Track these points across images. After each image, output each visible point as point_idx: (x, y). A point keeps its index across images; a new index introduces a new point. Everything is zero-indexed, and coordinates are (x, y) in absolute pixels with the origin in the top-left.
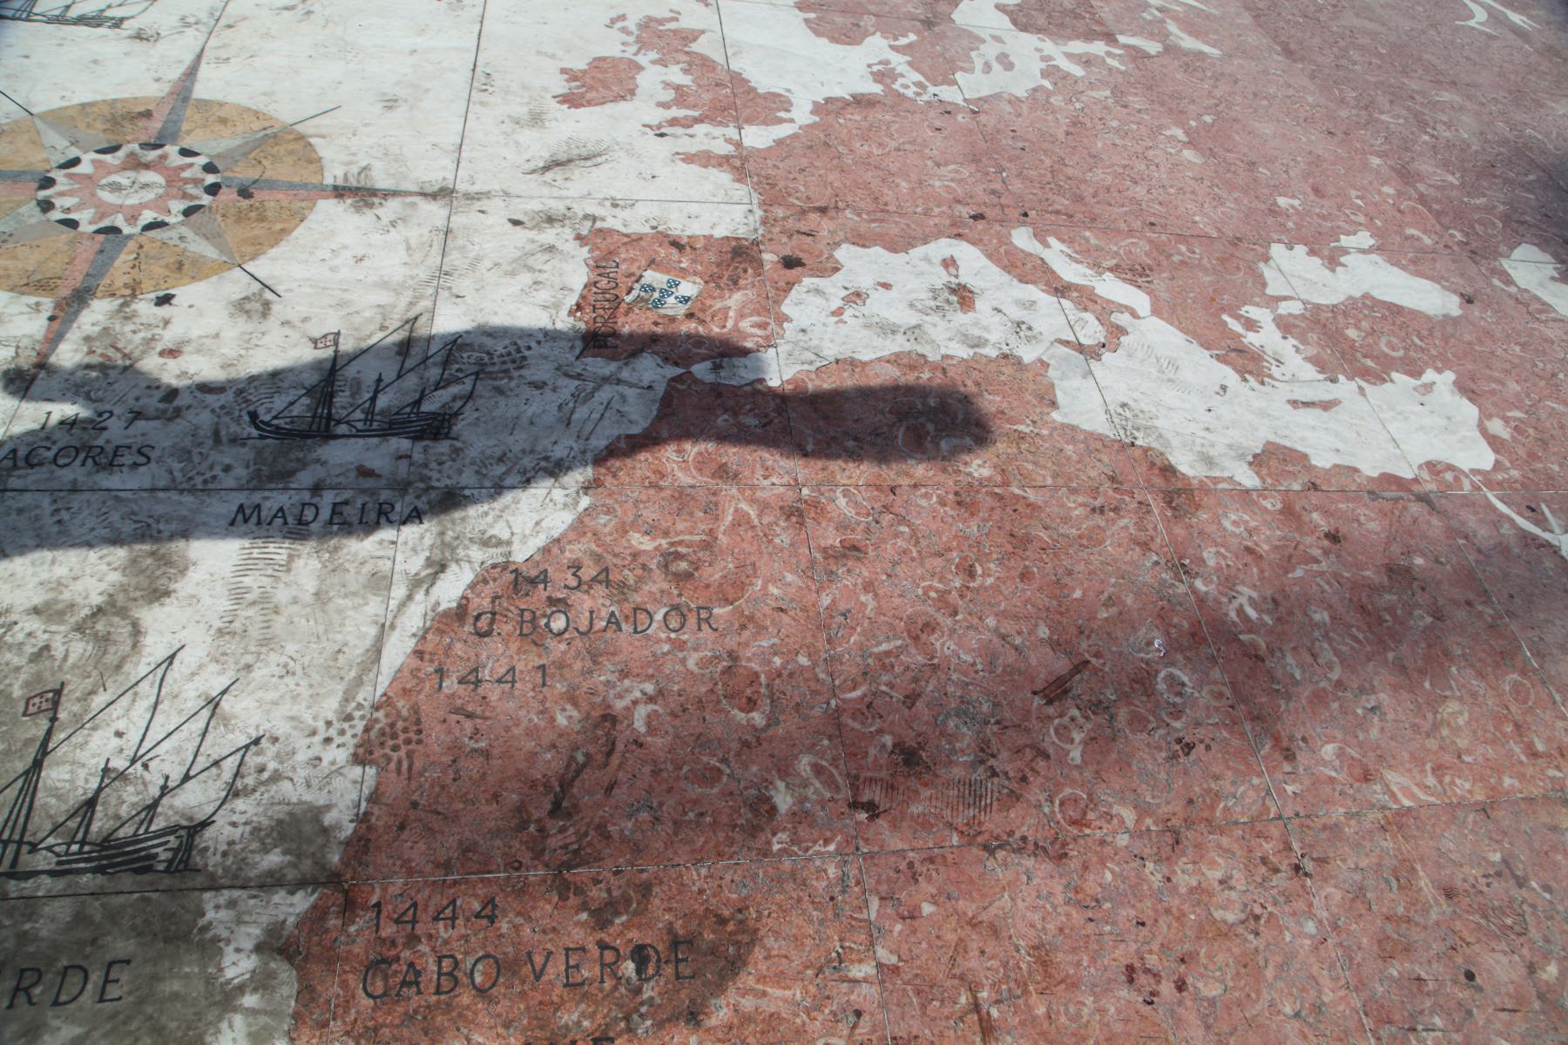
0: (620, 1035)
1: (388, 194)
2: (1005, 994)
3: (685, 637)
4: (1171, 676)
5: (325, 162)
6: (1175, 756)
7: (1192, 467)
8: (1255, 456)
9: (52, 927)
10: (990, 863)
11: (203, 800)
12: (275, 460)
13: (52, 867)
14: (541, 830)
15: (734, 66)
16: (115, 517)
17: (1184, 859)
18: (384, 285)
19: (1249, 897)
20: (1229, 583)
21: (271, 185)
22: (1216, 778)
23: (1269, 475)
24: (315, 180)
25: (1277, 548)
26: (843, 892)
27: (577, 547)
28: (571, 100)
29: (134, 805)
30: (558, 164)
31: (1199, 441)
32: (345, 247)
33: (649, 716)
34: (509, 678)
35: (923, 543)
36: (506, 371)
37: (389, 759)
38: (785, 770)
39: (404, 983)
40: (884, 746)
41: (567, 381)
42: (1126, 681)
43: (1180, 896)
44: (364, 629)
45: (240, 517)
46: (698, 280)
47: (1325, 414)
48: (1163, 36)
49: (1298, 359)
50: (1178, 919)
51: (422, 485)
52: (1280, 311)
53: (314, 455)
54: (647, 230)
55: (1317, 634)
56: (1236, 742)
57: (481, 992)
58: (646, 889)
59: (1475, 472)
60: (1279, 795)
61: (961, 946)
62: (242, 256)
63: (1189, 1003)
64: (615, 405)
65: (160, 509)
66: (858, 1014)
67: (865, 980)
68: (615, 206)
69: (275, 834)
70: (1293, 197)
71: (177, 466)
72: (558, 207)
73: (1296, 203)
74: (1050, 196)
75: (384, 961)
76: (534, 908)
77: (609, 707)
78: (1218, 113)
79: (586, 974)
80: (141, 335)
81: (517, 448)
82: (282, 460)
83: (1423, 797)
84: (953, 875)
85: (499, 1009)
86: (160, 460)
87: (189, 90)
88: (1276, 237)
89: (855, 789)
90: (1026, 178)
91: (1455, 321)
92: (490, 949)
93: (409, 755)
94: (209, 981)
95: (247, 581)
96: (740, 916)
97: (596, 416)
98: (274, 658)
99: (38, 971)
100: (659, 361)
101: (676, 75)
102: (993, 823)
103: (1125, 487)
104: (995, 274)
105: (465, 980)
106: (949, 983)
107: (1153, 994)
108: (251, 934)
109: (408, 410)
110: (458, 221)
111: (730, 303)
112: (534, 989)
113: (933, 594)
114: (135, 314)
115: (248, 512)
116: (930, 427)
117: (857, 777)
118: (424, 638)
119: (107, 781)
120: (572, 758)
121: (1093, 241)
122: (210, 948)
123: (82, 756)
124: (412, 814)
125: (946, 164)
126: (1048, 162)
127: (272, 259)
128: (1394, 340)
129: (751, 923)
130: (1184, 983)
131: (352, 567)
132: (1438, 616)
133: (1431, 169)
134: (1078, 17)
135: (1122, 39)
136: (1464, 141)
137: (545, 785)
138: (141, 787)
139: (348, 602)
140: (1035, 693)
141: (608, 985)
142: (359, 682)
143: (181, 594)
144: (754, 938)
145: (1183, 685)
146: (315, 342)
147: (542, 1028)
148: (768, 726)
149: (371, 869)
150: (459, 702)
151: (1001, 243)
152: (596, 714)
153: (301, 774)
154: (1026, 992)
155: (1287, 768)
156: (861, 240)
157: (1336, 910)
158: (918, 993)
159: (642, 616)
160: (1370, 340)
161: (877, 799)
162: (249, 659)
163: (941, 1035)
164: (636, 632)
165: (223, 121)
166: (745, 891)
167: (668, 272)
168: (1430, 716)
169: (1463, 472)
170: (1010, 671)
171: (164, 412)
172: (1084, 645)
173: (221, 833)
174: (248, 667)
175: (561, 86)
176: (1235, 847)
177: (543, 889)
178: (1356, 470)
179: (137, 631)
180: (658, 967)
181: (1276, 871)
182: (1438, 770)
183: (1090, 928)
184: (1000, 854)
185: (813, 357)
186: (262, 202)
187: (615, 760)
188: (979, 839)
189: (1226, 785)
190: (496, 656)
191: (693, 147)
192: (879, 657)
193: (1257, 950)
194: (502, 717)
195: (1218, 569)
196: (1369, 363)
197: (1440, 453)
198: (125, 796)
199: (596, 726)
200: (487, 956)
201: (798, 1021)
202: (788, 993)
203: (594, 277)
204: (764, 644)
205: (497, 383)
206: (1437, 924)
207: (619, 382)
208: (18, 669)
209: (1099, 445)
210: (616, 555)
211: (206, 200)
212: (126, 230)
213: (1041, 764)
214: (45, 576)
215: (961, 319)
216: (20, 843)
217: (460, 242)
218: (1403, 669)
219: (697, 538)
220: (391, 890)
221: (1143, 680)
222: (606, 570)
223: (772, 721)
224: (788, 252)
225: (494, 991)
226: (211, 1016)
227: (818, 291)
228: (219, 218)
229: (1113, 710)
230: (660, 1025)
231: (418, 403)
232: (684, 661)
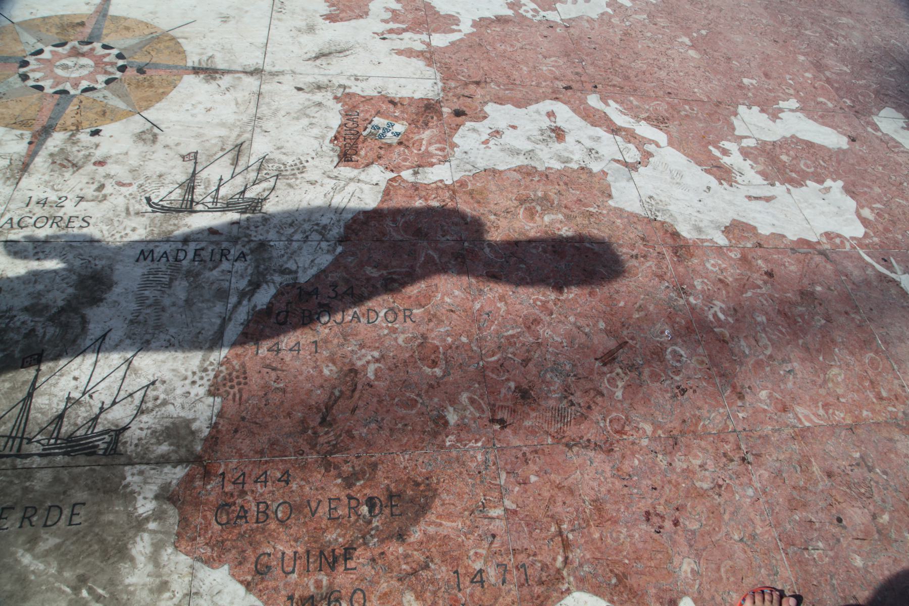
0: (359, 546)
2: (577, 526)
3: (397, 326)
4: (674, 351)
5: (187, 53)
6: (676, 396)
7: (689, 233)
8: (726, 227)
9: (41, 484)
10: (569, 454)
11: (123, 415)
12: (161, 225)
13: (40, 451)
14: (315, 433)
17: (680, 453)
18: (223, 124)
19: (716, 475)
20: (709, 299)
21: (156, 66)
22: (699, 408)
23: (734, 238)
24: (182, 64)
25: (737, 279)
26: (486, 469)
27: (335, 275)
28: (331, 18)
29: (85, 418)
31: (693, 218)
32: (200, 103)
33: (376, 370)
36: (294, 174)
37: (229, 393)
38: (453, 401)
39: (238, 517)
40: (510, 388)
41: (329, 180)
42: (648, 353)
43: (677, 473)
44: (213, 320)
45: (142, 257)
46: (405, 123)
47: (767, 204)
49: (752, 172)
50: (675, 486)
51: (246, 239)
52: (743, 145)
53: (184, 222)
54: (375, 94)
55: (759, 328)
56: (711, 389)
57: (282, 522)
58: (374, 466)
59: (853, 238)
60: (734, 418)
61: (552, 500)
62: (140, 108)
63: (680, 533)
64: (357, 194)
66: (494, 536)
67: (498, 518)
68: (357, 80)
69: (164, 435)
70: (752, 78)
71: (105, 228)
72: (323, 80)
73: (754, 82)
74: (610, 76)
75: (227, 505)
76: (311, 476)
77: (353, 365)
79: (340, 512)
80: (83, 153)
82: (165, 225)
83: (816, 420)
84: (548, 460)
85: (292, 531)
86: (95, 225)
87: (107, 10)
88: (741, 102)
89: (493, 411)
90: (596, 66)
91: (844, 152)
92: (287, 499)
93: (240, 391)
94: (130, 515)
95: (147, 293)
96: (427, 482)
98: (162, 336)
99: (34, 507)
100: (382, 169)
102: (571, 431)
103: (650, 244)
104: (577, 121)
105: (272, 516)
106: (545, 520)
107: (660, 527)
108: (152, 489)
109: (237, 196)
110: (265, 88)
111: (423, 136)
112: (311, 520)
113: (539, 303)
114: (78, 141)
115: (146, 254)
116: (538, 208)
117: (494, 405)
119: (69, 404)
120: (332, 393)
121: (635, 103)
122: (130, 497)
123: (54, 390)
124: (242, 424)
125: (550, 57)
126: (609, 56)
127: (157, 110)
128: (809, 162)
129: (434, 486)
130: (678, 521)
132: (829, 319)
133: (834, 63)
136: (854, 47)
137: (317, 408)
138: (89, 408)
139: (204, 305)
140: (596, 359)
141: (353, 519)
143: (110, 300)
144: (435, 494)
145: (681, 356)
146: (183, 157)
147: (316, 542)
148: (444, 376)
149: (219, 454)
150: (268, 361)
151: (581, 103)
152: (346, 368)
153: (179, 401)
154: (588, 525)
155: (740, 403)
156: (500, 101)
157: (765, 483)
158: (528, 525)
159: (372, 314)
160: (794, 162)
161: (505, 418)
162: (148, 337)
163: (540, 548)
164: (369, 322)
165: (127, 29)
166: (430, 468)
167: (387, 118)
168: (822, 376)
169: (846, 238)
170: (582, 346)
171: (97, 197)
172: (625, 333)
173: (134, 434)
176: (709, 447)
177: (316, 466)
178: (784, 236)
179: (84, 322)
180: (381, 512)
181: (732, 460)
182: (826, 406)
183: (625, 491)
184: (575, 449)
185: (471, 168)
186: (151, 76)
187: (357, 395)
188: (563, 440)
189: (704, 412)
191: (402, 46)
193: (719, 504)
194: (292, 370)
195: (703, 291)
196: (794, 175)
197: (833, 226)
198: (79, 413)
199: (346, 375)
200: (285, 502)
201: (460, 539)
202: (454, 524)
203: (344, 121)
204: (442, 330)
205: (289, 181)
206: (822, 491)
207: (359, 181)
208: (17, 342)
209: (635, 220)
210: (357, 280)
211: (118, 75)
213: (599, 399)
214: (31, 290)
215: (557, 147)
216: (22, 438)
218: (807, 349)
219: (404, 270)
220: (230, 465)
222: (352, 287)
223: (446, 373)
224: (457, 107)
225: (288, 522)
228: (126, 86)
229: (641, 370)
230: (382, 541)
231: (243, 192)
232: (396, 339)
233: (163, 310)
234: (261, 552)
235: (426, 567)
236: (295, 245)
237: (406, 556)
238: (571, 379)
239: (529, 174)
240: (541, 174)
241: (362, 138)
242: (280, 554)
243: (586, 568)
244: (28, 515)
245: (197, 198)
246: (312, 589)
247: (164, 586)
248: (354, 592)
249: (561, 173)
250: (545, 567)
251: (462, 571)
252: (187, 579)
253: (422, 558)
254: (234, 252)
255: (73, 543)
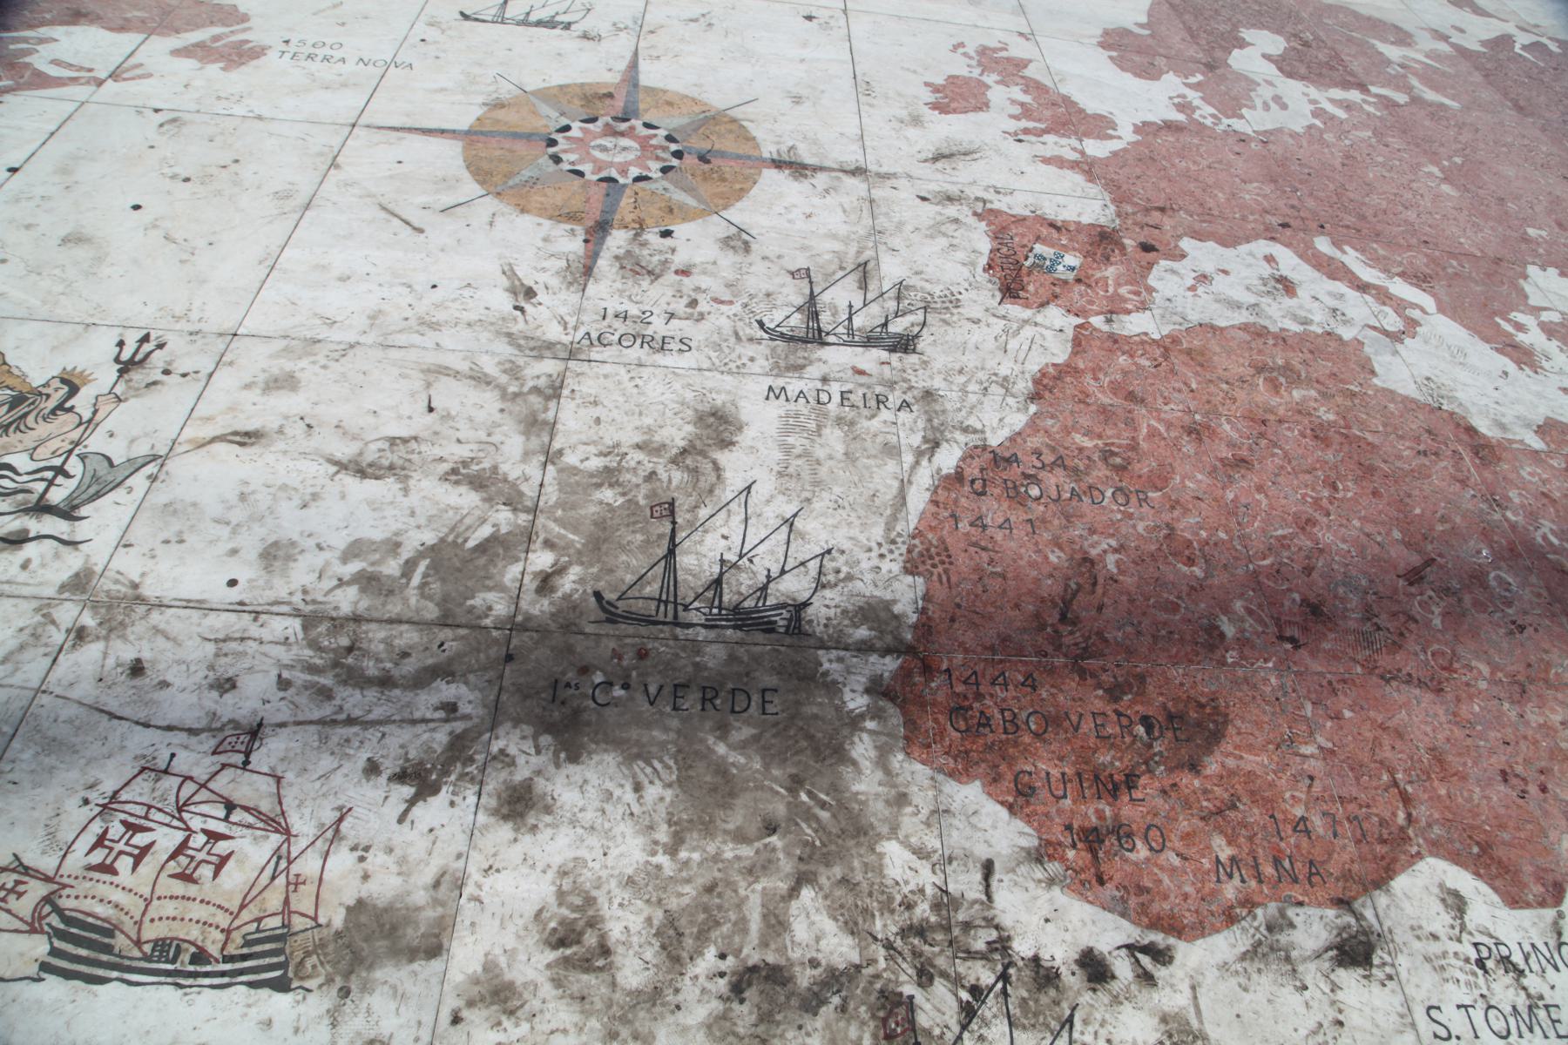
0: (1143, 773)
1: (816, 169)
4: (1498, 578)
5: (759, 140)
10: (1388, 689)
14: (1056, 631)
15: (1063, 90)
16: (677, 386)
18: (834, 237)
21: (722, 155)
30: (944, 157)
34: (1006, 525)
35: (1294, 463)
38: (1226, 610)
39: (979, 724)
41: (995, 320)
48: (1408, 89)
54: (1027, 213)
56: (1558, 630)
57: (1037, 735)
58: (1141, 679)
61: (1377, 742)
64: (1038, 340)
65: (709, 384)
66: (1311, 778)
67: (1312, 756)
71: (713, 355)
72: (953, 190)
73: (1544, 233)
75: (961, 708)
78: (1465, 156)
81: (971, 365)
90: (1317, 198)
93: (946, 571)
94: (838, 709)
97: (1025, 347)
98: (824, 494)
101: (1017, 93)
102: (1385, 661)
108: (860, 681)
110: (877, 193)
116: (1282, 380)
118: (935, 492)
120: (1067, 586)
121: (1381, 252)
122: (833, 688)
123: (703, 549)
125: (1251, 182)
131: (868, 438)
134: (1332, 68)
135: (1373, 89)
139: (871, 462)
142: (894, 518)
146: (792, 274)
148: (1206, 578)
149: (936, 646)
152: (1078, 556)
153: (868, 577)
154: (1429, 778)
156: (1199, 236)
158: (1352, 769)
159: (1096, 493)
163: (1373, 799)
165: (670, 104)
166: (1213, 688)
167: (1052, 246)
174: (808, 500)
175: (931, 98)
179: (717, 468)
180: (1162, 734)
183: (1469, 741)
184: (1394, 684)
187: (1099, 590)
189: (1554, 656)
190: (994, 509)
191: (1048, 152)
192: (1279, 539)
195: (1523, 506)
199: (1080, 565)
200: (1036, 712)
202: (1258, 759)
203: (995, 245)
207: (1036, 324)
208: (638, 486)
211: (675, 162)
212: (622, 181)
213: (1413, 626)
214: (638, 423)
215: (1288, 302)
217: (884, 210)
221: (1477, 577)
226: (846, 732)
227: (1173, 272)
230: (1170, 770)
231: (885, 325)
232: (1134, 526)
233: (818, 463)
234: (1018, 768)
235: (1234, 807)
236: (972, 398)
237: (1205, 791)
238: (1371, 598)
239: (1259, 335)
240: (1276, 336)
241: (1024, 270)
242: (1043, 774)
243: (1437, 830)
244: (709, 696)
245: (826, 327)
246: (1094, 819)
247: (902, 799)
248: (1148, 828)
249: (1303, 338)
250: (1383, 823)
251: (1279, 816)
252: (931, 793)
253: (1226, 796)
254: (894, 399)
255: (774, 736)
